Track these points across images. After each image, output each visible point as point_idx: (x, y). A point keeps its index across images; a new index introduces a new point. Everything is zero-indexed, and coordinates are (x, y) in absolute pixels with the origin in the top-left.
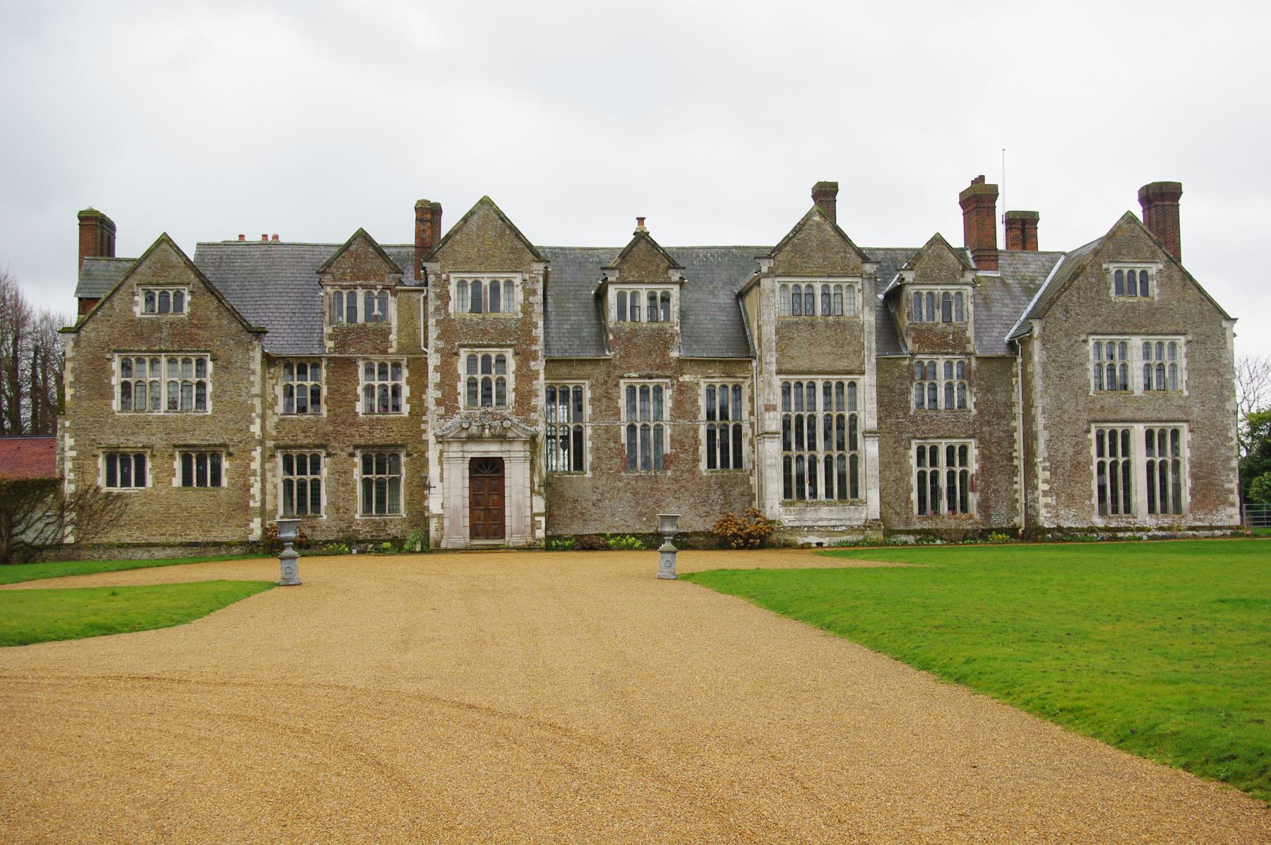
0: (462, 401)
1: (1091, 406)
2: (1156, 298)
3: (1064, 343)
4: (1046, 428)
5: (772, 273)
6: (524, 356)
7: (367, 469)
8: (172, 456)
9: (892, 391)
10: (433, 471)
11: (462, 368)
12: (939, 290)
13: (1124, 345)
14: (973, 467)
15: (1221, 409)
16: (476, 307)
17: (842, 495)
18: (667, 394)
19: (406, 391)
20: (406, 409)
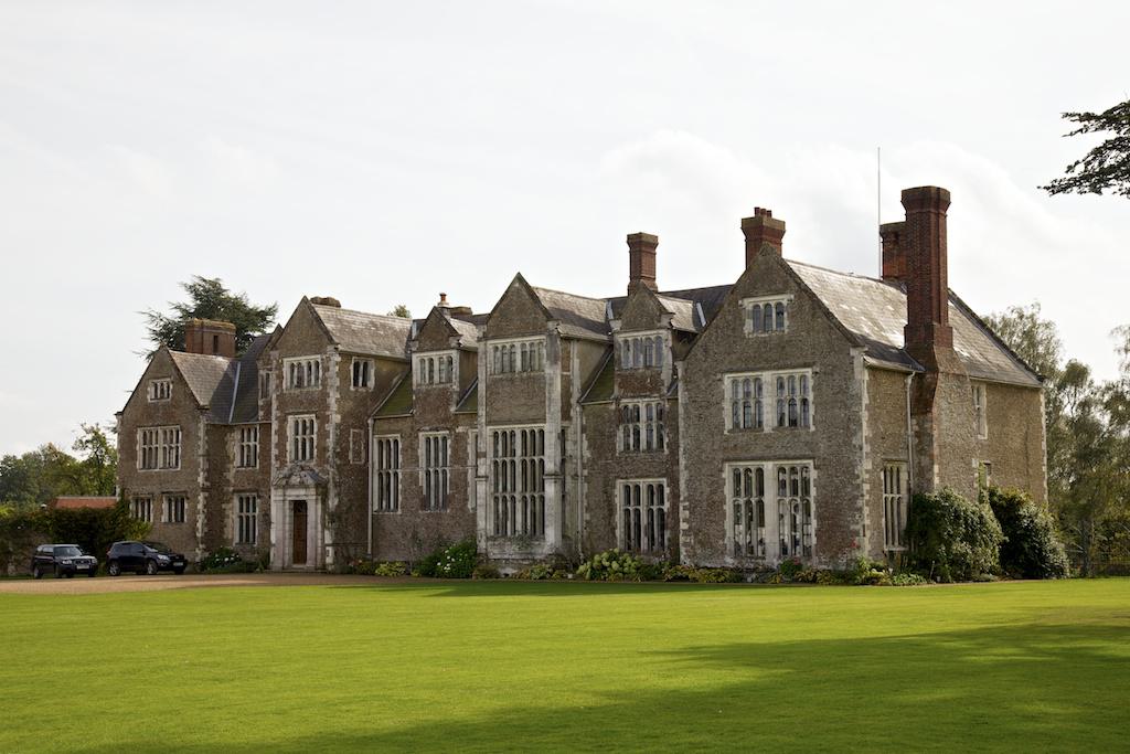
1: (725, 444)
2: (786, 331)
3: (703, 383)
4: (686, 468)
8: (162, 499)
9: (602, 434)
11: (290, 432)
12: (641, 335)
13: (757, 379)
14: (666, 506)
15: (848, 443)
16: (300, 384)
18: (449, 442)
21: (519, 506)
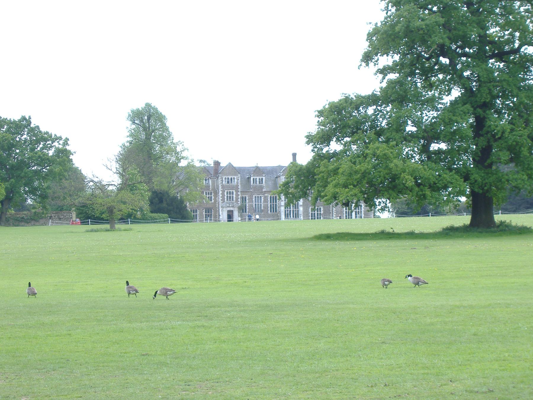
0: (226, 200)
5: (282, 175)
6: (237, 192)
7: (206, 212)
10: (221, 213)
11: (226, 194)
14: (322, 212)
16: (228, 182)
17: (296, 217)
18: (262, 198)
19: (213, 198)
20: (213, 201)
21: (292, 212)
